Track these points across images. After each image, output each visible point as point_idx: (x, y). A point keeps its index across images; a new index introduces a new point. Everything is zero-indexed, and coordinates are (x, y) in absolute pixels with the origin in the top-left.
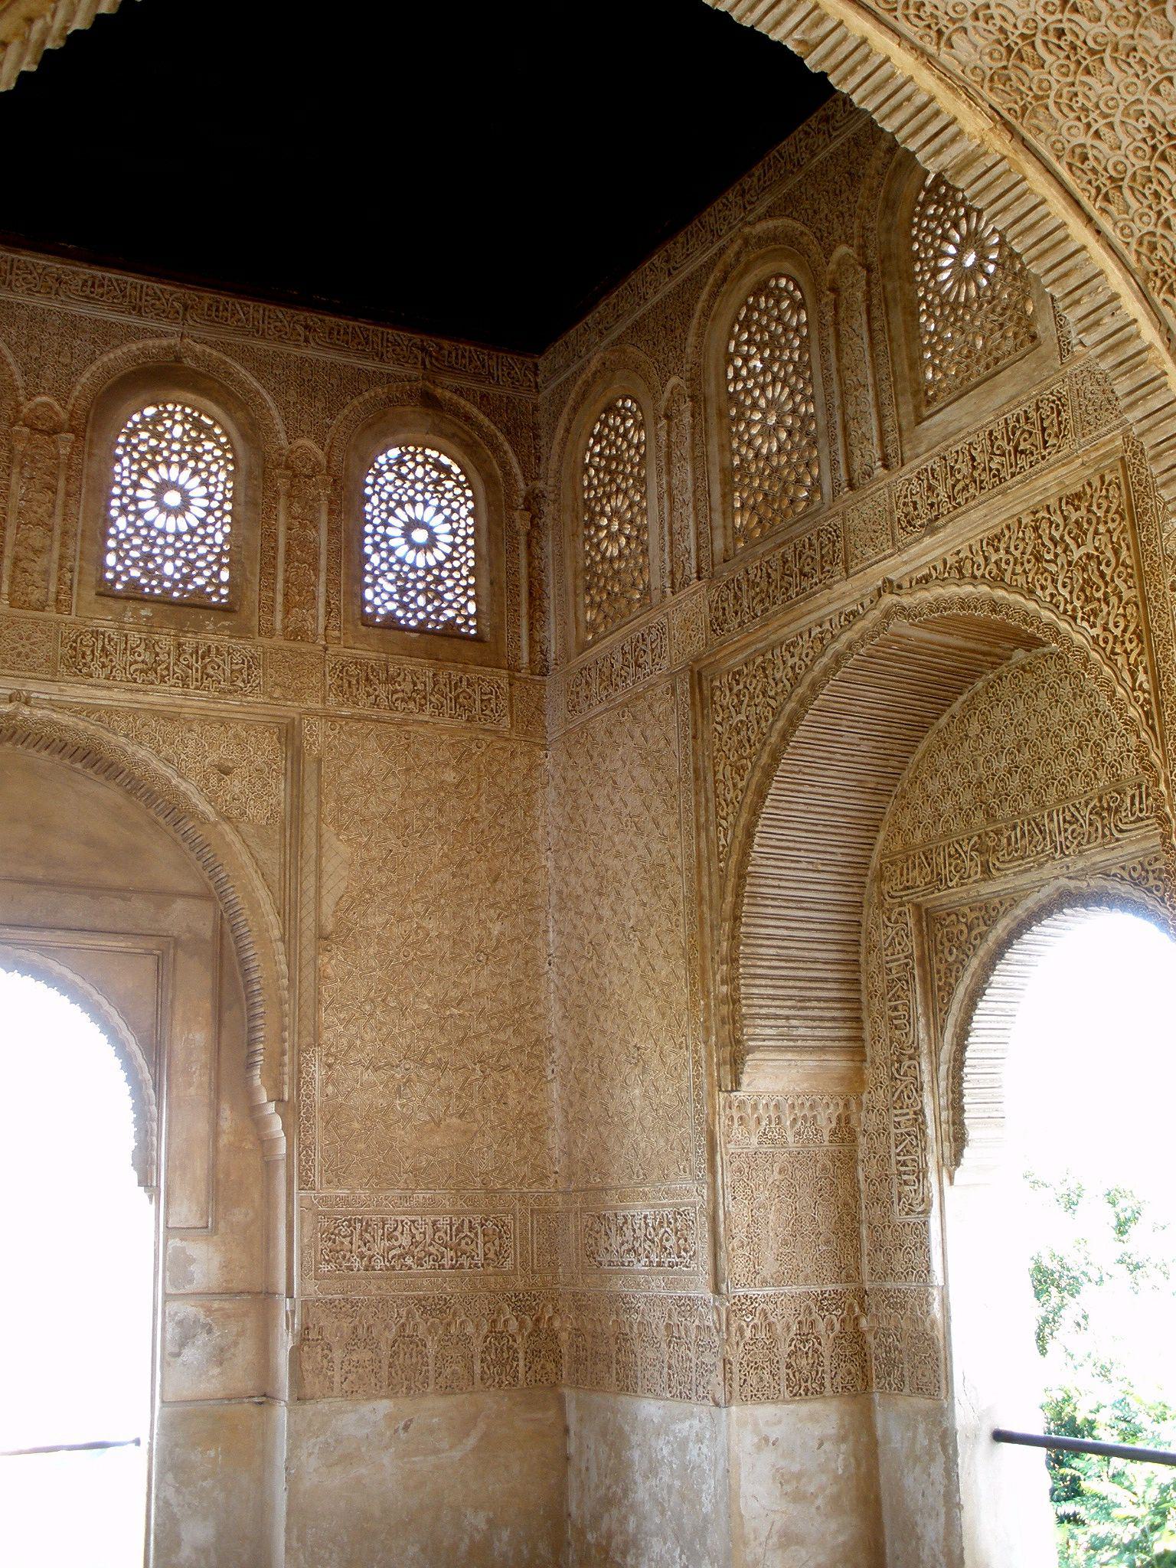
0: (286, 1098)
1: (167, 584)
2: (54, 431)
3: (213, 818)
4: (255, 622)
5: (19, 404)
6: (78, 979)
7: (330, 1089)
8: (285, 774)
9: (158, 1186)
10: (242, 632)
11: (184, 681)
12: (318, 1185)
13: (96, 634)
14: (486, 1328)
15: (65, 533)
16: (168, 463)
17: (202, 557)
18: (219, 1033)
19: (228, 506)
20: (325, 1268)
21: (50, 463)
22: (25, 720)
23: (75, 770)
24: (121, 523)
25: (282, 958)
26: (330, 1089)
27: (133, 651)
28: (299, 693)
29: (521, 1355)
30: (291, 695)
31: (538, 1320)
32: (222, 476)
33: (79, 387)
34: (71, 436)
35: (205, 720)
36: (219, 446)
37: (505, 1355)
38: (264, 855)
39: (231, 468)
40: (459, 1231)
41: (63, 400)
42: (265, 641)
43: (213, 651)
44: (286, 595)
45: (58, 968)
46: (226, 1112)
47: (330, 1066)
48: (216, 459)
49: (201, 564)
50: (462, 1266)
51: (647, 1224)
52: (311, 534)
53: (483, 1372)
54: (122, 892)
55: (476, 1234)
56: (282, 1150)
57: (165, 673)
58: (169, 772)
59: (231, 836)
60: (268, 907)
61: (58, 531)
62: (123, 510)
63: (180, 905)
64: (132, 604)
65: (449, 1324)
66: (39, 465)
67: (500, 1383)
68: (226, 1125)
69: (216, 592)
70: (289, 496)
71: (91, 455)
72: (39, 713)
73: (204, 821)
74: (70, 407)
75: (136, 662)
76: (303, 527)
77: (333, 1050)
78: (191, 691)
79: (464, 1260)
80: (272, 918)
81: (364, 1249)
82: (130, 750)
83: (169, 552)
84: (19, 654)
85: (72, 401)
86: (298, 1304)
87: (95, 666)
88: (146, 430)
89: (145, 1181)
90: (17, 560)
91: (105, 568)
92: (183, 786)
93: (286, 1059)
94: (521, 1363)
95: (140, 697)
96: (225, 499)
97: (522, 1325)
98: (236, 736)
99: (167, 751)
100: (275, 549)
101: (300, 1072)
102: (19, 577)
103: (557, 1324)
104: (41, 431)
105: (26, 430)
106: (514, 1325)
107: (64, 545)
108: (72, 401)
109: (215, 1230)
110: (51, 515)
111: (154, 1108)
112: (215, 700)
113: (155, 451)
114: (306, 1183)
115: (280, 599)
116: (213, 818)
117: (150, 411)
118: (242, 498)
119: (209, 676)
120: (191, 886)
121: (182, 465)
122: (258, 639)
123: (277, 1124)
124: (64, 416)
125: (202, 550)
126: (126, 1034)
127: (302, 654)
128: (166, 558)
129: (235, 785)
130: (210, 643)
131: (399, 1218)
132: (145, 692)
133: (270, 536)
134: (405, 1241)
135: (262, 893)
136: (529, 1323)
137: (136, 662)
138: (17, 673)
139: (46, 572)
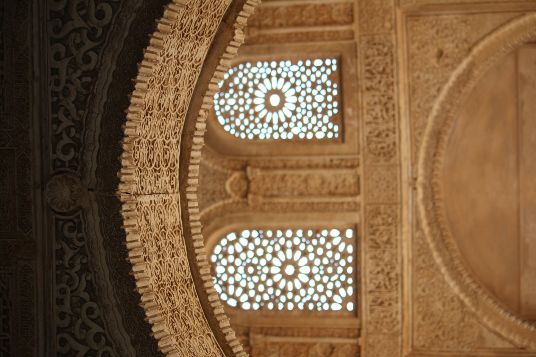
1: (330, 98)
2: (246, 178)
4: (345, 42)
5: (234, 202)
8: (438, 15)
10: (354, 50)
11: (389, 85)
13: (369, 142)
15: (310, 167)
16: (253, 106)
17: (309, 78)
19: (274, 64)
21: (267, 180)
22: (426, 178)
23: (449, 141)
24: (295, 131)
27: (376, 118)
28: (386, 12)
30: (388, 17)
32: (254, 70)
33: (216, 167)
34: (249, 169)
35: (410, 69)
36: (235, 74)
38: (489, 26)
39: (248, 65)
41: (225, 177)
42: (357, 35)
43: (368, 68)
44: (324, 24)
48: (245, 75)
49: (313, 78)
52: (282, 11)
54: (519, 105)
57: (386, 97)
58: (445, 89)
59: (480, 47)
60: (521, 21)
61: (309, 172)
62: (288, 130)
63: (523, 70)
64: (347, 121)
66: (269, 185)
69: (330, 67)
70: (260, 27)
71: (257, 155)
72: (421, 171)
73: (472, 66)
74: (229, 172)
75: (382, 116)
76: (279, 16)
78: (395, 80)
82: (434, 113)
83: (309, 99)
84: (388, 187)
85: (225, 171)
87: (389, 141)
88: (234, 122)
90: (331, 194)
91: (326, 138)
95: (402, 111)
96: (269, 66)
98: (418, 48)
99: (433, 91)
100: (296, 34)
102: (340, 190)
104: (248, 187)
105: (250, 196)
107: (317, 167)
108: (225, 171)
110: (300, 176)
112: (398, 64)
113: (247, 114)
115: (328, 28)
117: (221, 120)
118: (267, 56)
119: (384, 69)
120: (510, 63)
121: (253, 96)
122: (357, 39)
124: (236, 175)
125: (304, 78)
127: (361, 11)
128: (313, 100)
129: (449, 47)
130: (363, 71)
132: (399, 108)
133: (288, 38)
135: (513, 25)
137: (382, 116)
138: (399, 188)
139: (335, 176)
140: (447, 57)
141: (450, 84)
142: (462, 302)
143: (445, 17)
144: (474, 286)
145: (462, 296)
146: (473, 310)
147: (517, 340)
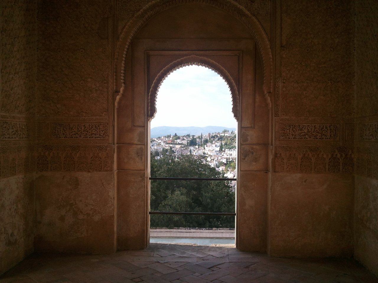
0: (272, 92)
3: (250, 15)
6: (217, 64)
7: (284, 89)
9: (239, 116)
12: (280, 115)
14: (330, 156)
18: (255, 76)
20: (282, 138)
25: (270, 53)
26: (284, 89)
29: (341, 164)
31: (346, 155)
37: (336, 164)
40: (322, 129)
45: (211, 61)
46: (257, 97)
47: (284, 83)
50: (323, 138)
51: (375, 127)
53: (329, 168)
55: (328, 130)
56: (270, 106)
59: (255, 20)
65: (319, 154)
67: (334, 172)
68: (257, 100)
77: (285, 78)
79: (323, 137)
80: (268, 42)
81: (293, 133)
86: (274, 148)
89: (235, 116)
92: (241, 7)
93: (272, 81)
94: (341, 167)
97: (341, 156)
101: (275, 85)
103: (353, 156)
106: (339, 156)
109: (254, 128)
111: (238, 96)
114: (277, 115)
116: (250, 15)
123: (269, 99)
126: (230, 77)
131: (304, 125)
134: (306, 131)
135: (265, 36)
136: (344, 156)
140: (251, 5)
141: (239, 6)
142: (139, 10)
143: (270, 4)
144: (146, 16)
145: (142, 10)
146: (136, 16)
147: (122, 36)
